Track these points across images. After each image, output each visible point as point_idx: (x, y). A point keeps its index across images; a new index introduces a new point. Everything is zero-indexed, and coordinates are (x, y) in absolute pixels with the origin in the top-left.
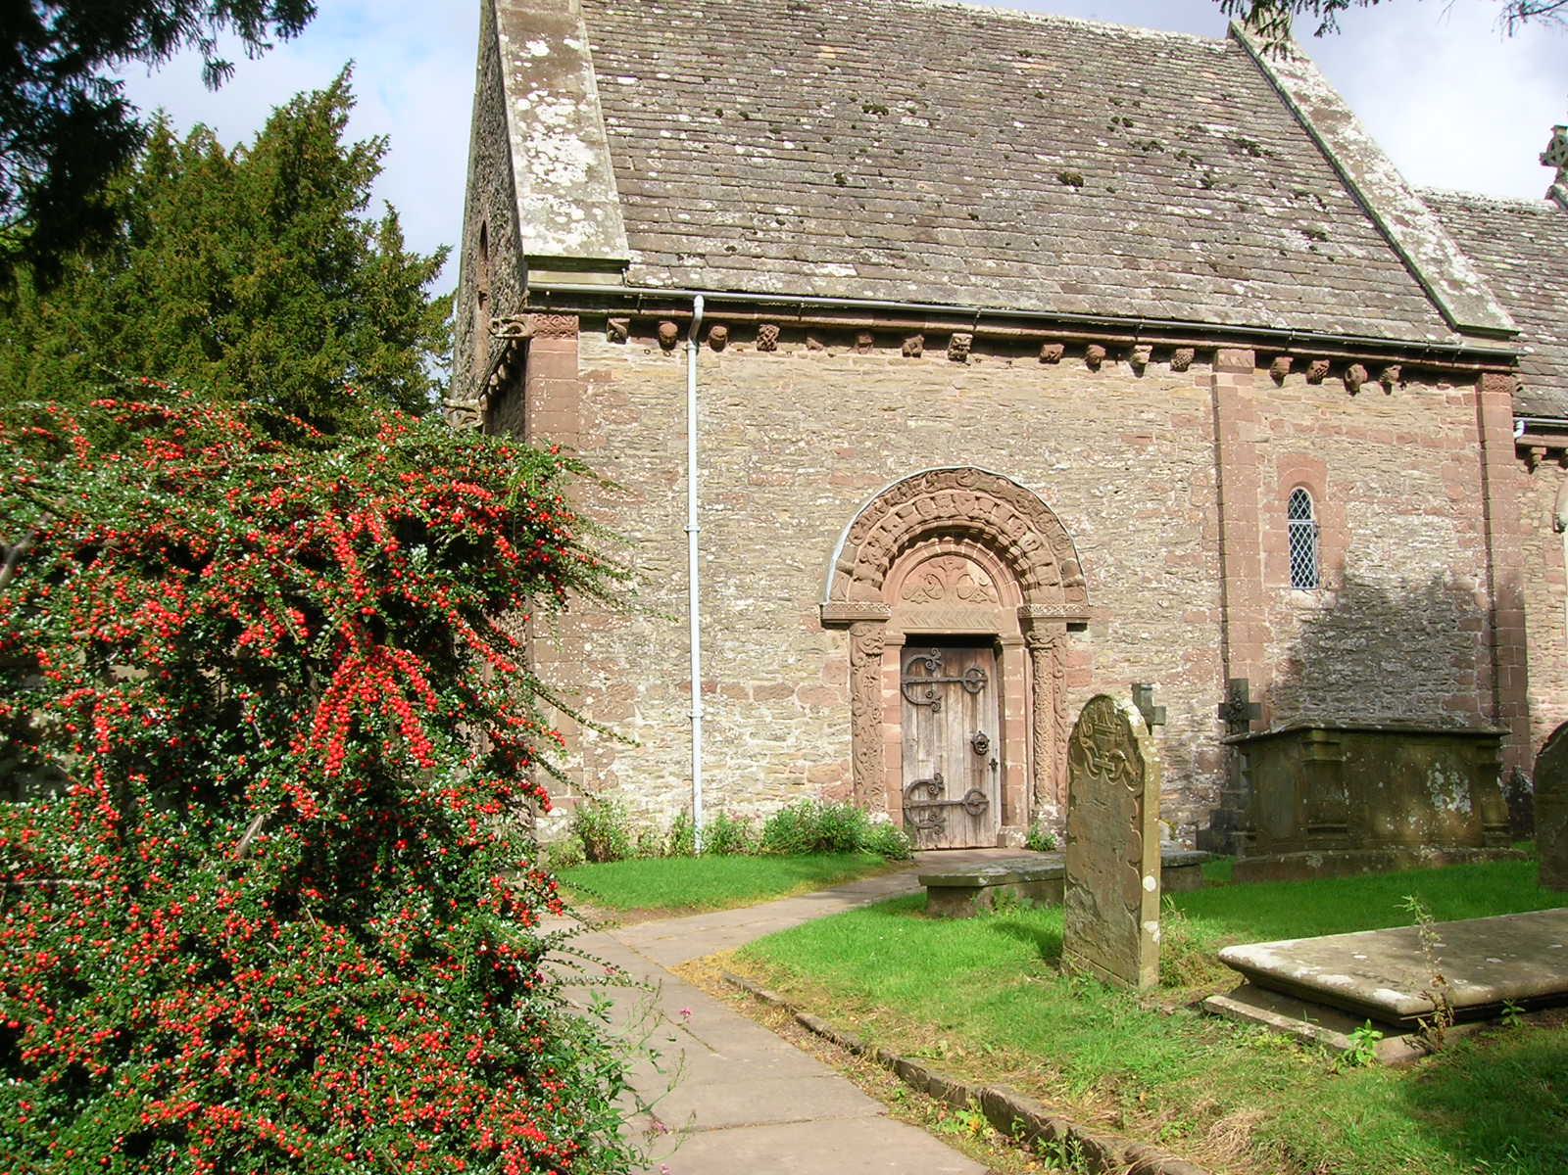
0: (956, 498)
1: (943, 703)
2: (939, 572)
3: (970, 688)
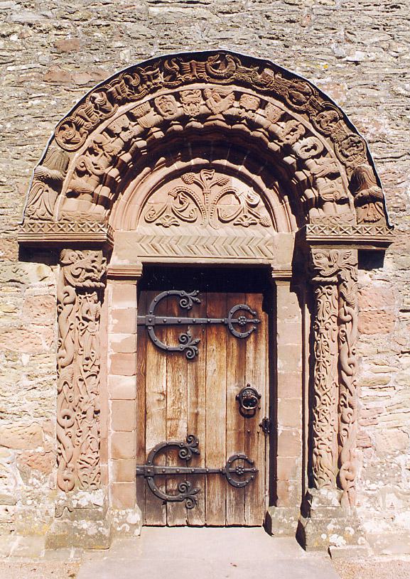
0: (208, 93)
2: (194, 189)
3: (237, 333)
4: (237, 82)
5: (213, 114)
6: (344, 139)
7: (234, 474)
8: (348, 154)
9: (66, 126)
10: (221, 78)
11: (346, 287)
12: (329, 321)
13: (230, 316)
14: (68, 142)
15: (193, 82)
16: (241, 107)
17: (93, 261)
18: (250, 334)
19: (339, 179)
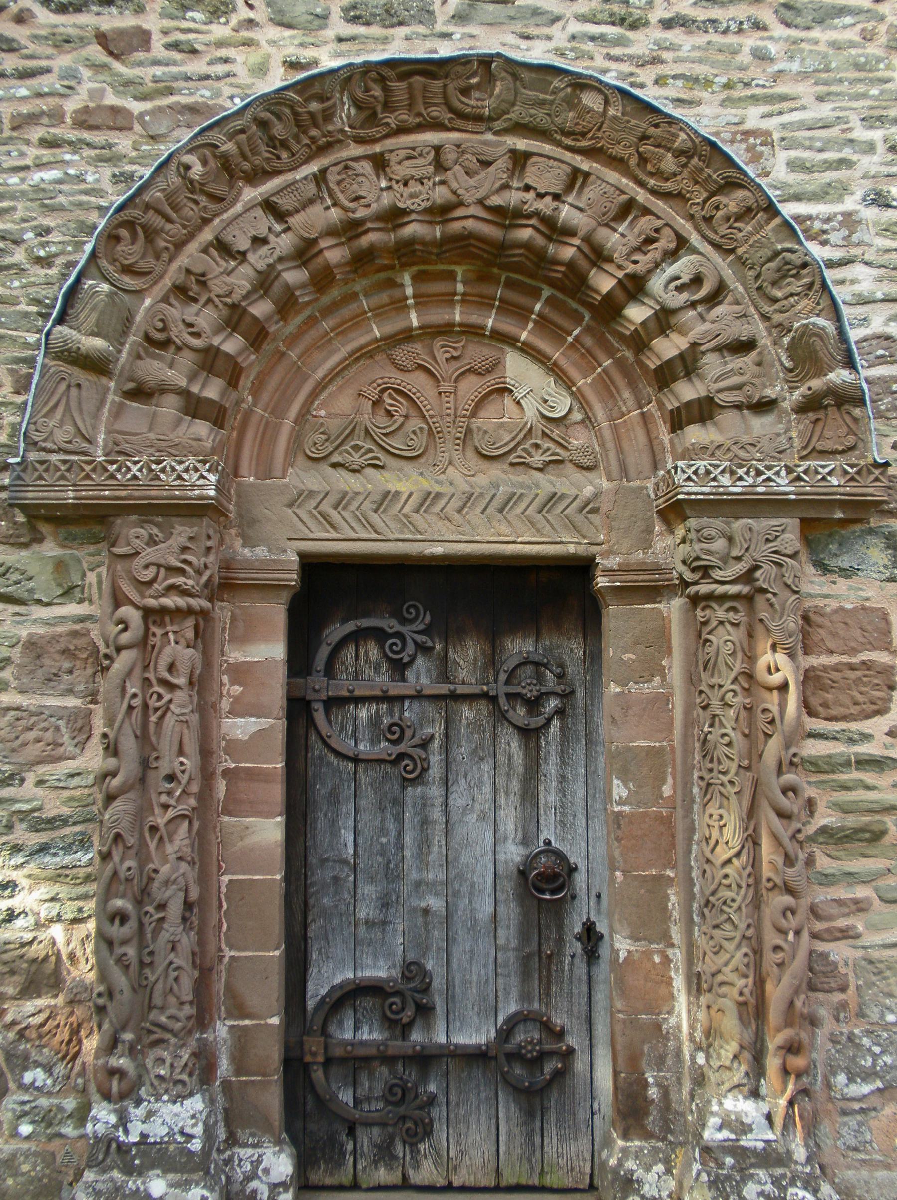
0: (450, 156)
1: (436, 760)
2: (417, 383)
3: (520, 713)
4: (520, 128)
5: (461, 204)
6: (770, 260)
7: (514, 1056)
8: (779, 294)
9: (124, 233)
10: (478, 118)
11: (772, 605)
12: (733, 687)
13: (503, 677)
14: (127, 270)
15: (420, 127)
16: (527, 188)
17: (185, 549)
18: (549, 721)
19: (754, 354)
